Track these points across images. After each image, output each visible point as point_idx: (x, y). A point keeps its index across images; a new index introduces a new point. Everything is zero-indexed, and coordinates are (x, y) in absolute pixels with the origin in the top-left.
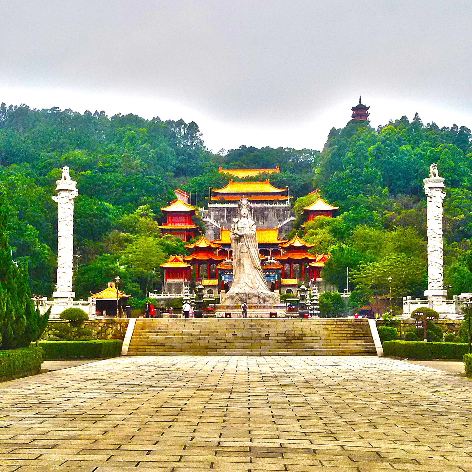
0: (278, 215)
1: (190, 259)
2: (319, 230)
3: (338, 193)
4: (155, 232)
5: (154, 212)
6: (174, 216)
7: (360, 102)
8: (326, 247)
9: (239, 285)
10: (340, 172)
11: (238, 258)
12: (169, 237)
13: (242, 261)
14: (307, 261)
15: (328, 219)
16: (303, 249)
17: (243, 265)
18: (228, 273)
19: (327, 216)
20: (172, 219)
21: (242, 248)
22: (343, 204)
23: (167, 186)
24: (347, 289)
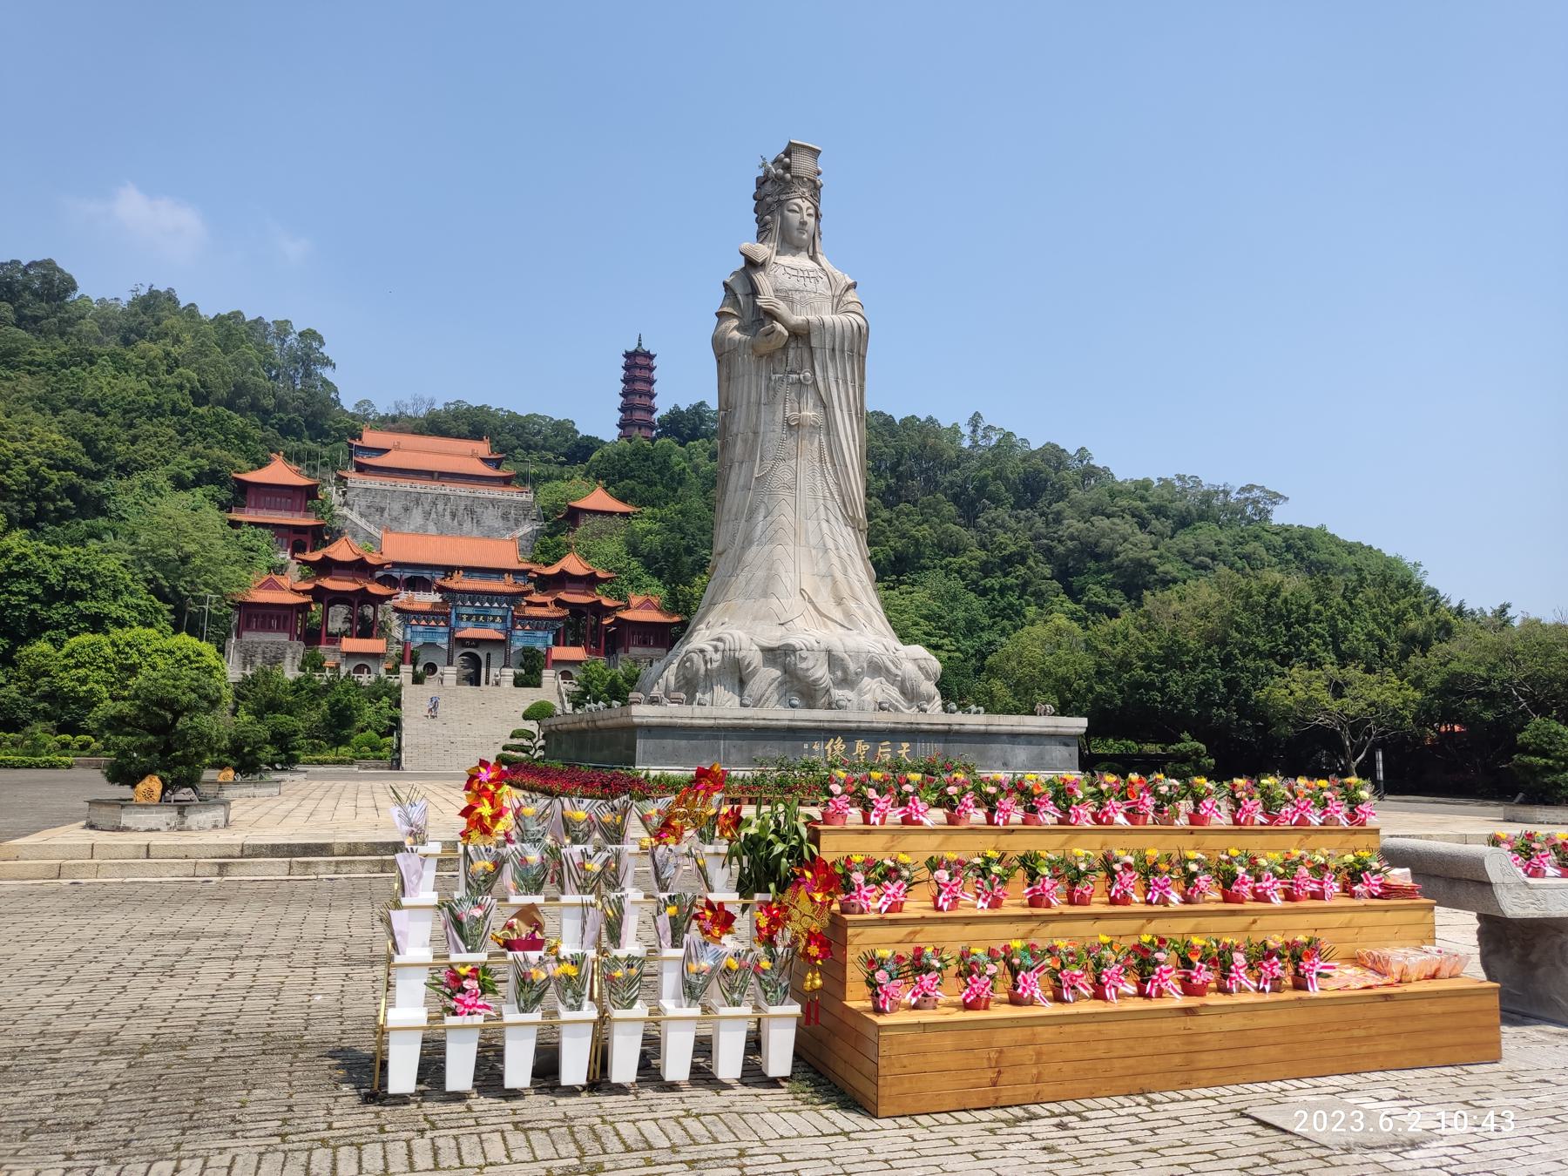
0: (505, 517)
1: (310, 586)
7: (640, 345)
14: (598, 609)
16: (590, 581)
18: (423, 622)
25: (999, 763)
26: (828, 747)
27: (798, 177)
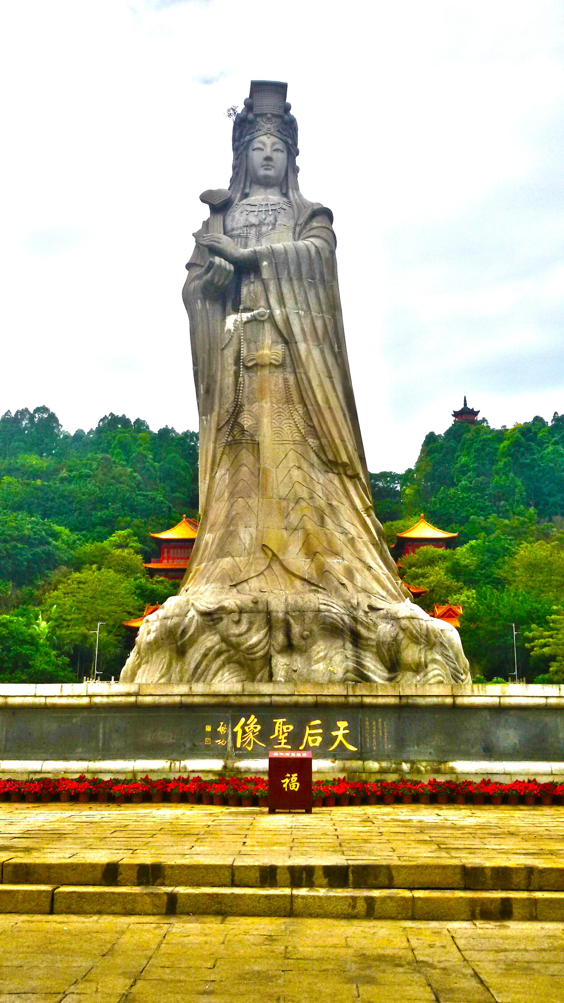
2: (428, 569)
3: (452, 514)
4: (137, 573)
5: (141, 542)
6: (172, 548)
7: (465, 404)
8: (442, 599)
9: (226, 562)
10: (448, 489)
11: (228, 405)
12: (162, 582)
13: (246, 421)
15: (441, 551)
17: (256, 446)
19: (440, 547)
20: (168, 552)
21: (254, 341)
22: (465, 529)
23: (169, 507)
24: (516, 673)
25: (478, 748)
26: (238, 729)
27: (261, 115)
